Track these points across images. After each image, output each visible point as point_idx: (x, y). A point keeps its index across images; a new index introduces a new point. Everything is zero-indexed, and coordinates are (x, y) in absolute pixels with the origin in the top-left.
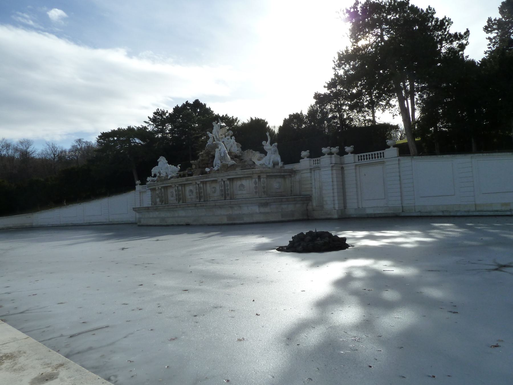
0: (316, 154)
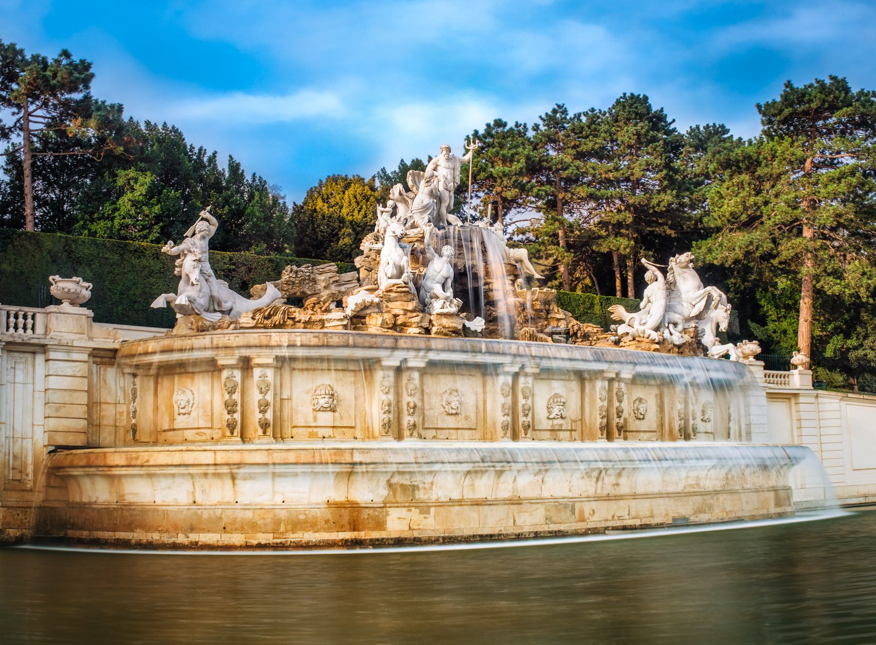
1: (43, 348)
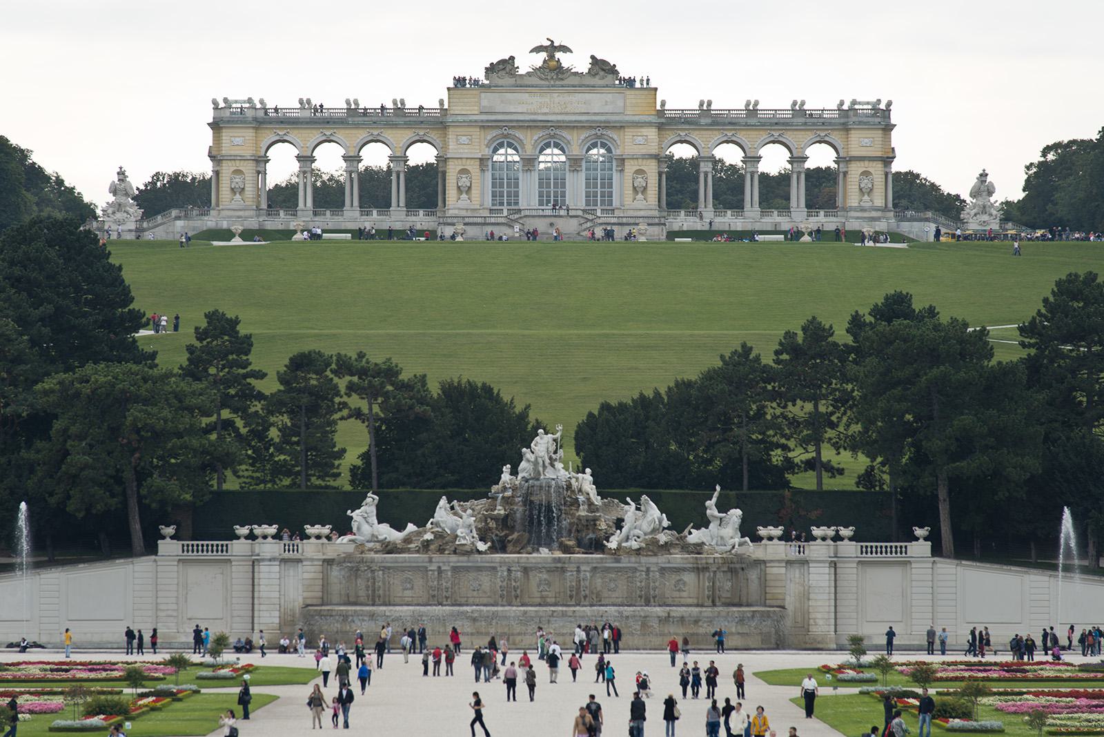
0: (797, 532)
1: (299, 561)
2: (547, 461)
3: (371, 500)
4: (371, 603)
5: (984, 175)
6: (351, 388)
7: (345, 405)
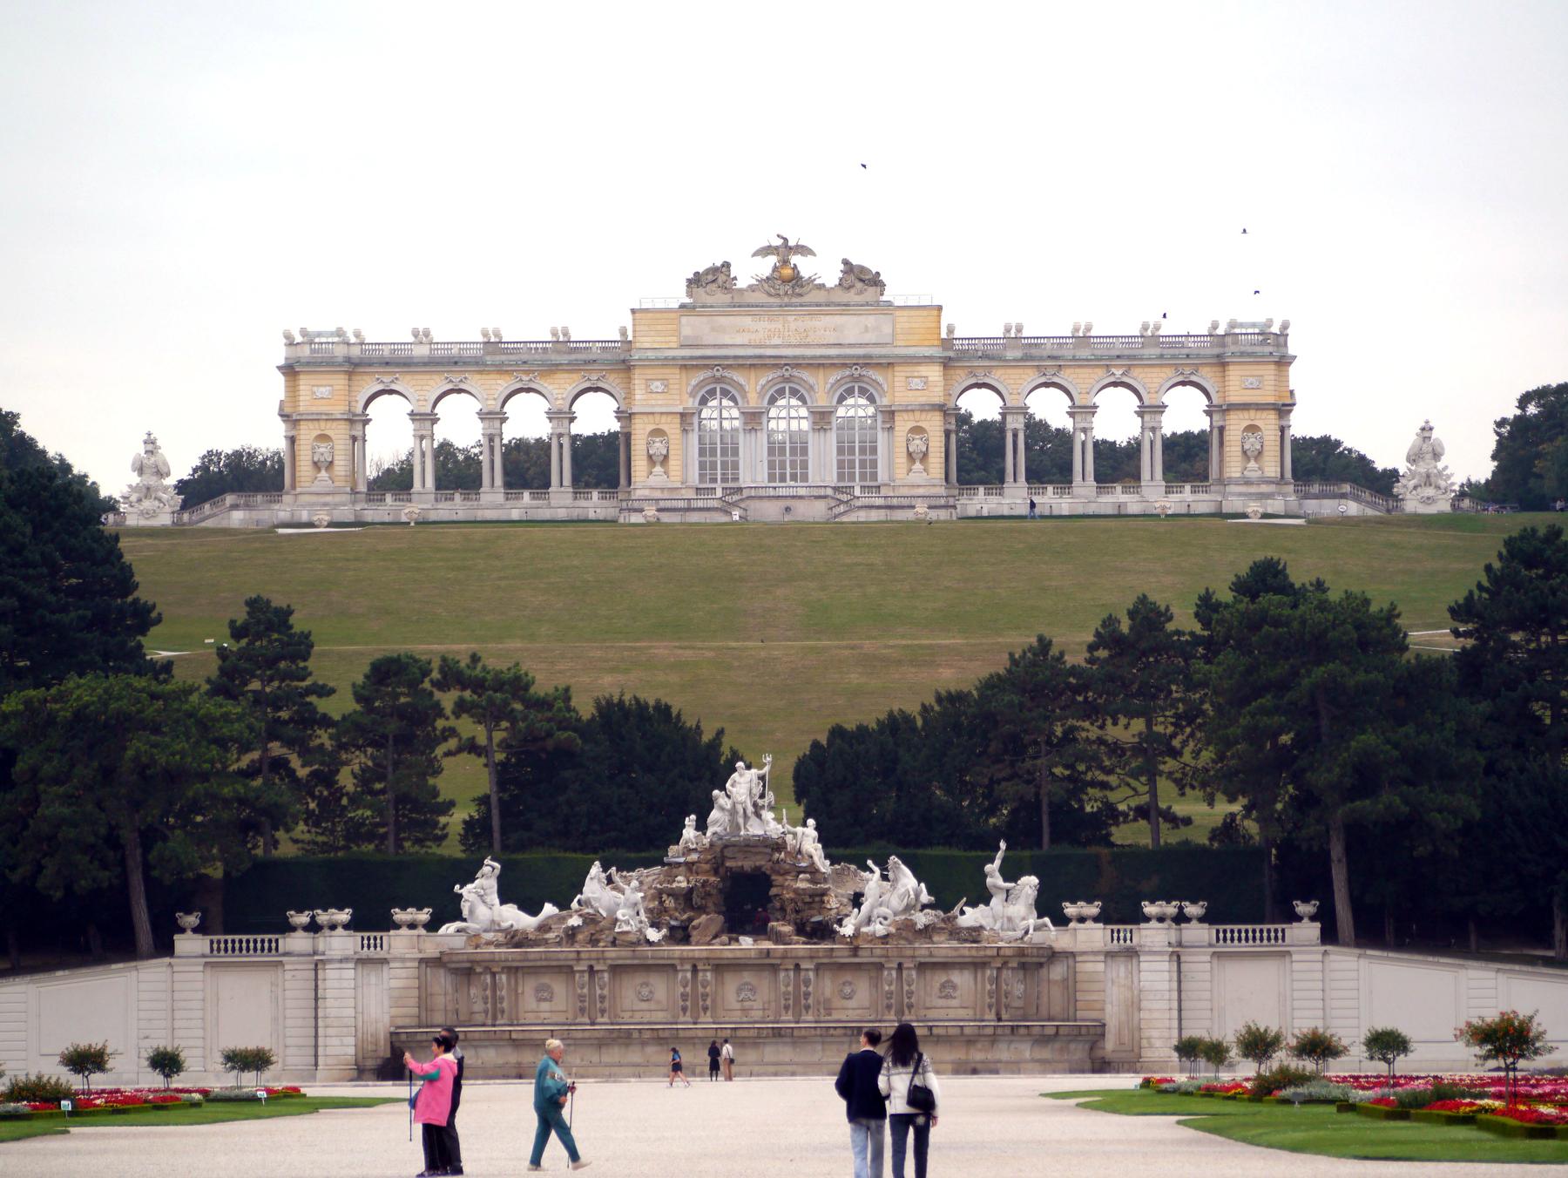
0: (1122, 912)
1: (384, 961)
2: (750, 809)
3: (490, 869)
4: (489, 1022)
5: (1427, 429)
6: (461, 708)
7: (452, 732)
